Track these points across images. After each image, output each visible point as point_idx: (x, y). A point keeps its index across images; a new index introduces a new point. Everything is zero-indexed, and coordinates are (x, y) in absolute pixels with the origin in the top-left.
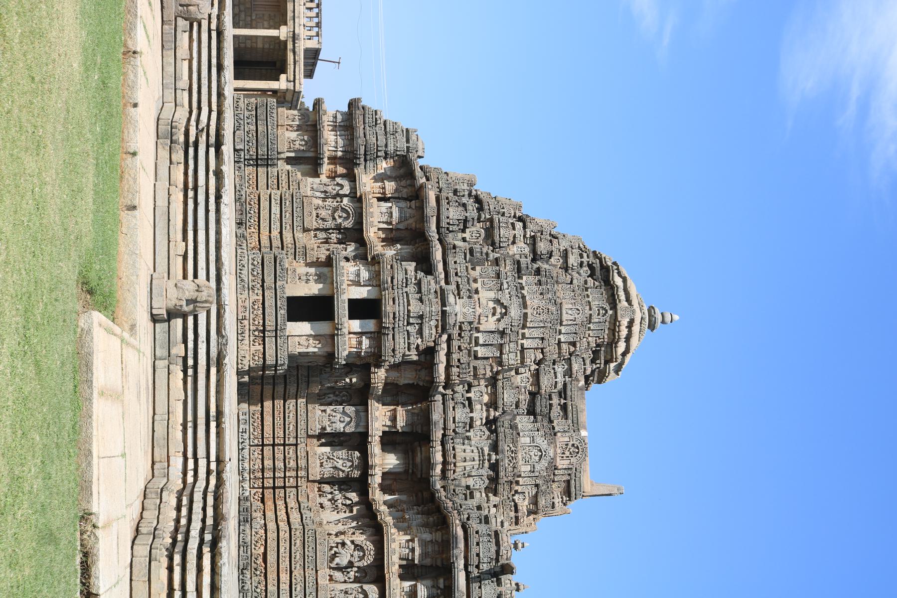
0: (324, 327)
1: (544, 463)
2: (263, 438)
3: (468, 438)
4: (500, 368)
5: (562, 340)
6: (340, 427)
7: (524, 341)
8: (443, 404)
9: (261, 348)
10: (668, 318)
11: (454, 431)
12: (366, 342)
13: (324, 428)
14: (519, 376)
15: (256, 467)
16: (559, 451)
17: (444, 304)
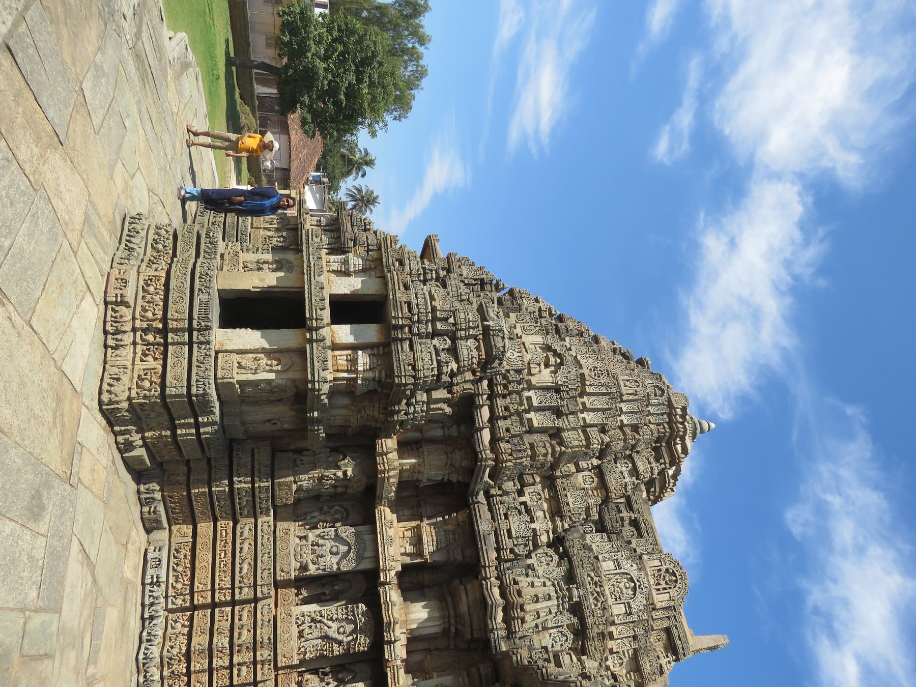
0: (288, 337)
1: (640, 600)
2: (192, 594)
3: (530, 567)
4: (563, 449)
5: (625, 422)
6: (331, 563)
7: (585, 415)
8: (490, 510)
9: (158, 365)
10: (706, 427)
11: (512, 551)
12: (363, 359)
13: (304, 568)
14: (580, 475)
15: (175, 651)
16: (652, 581)
17: (484, 319)
